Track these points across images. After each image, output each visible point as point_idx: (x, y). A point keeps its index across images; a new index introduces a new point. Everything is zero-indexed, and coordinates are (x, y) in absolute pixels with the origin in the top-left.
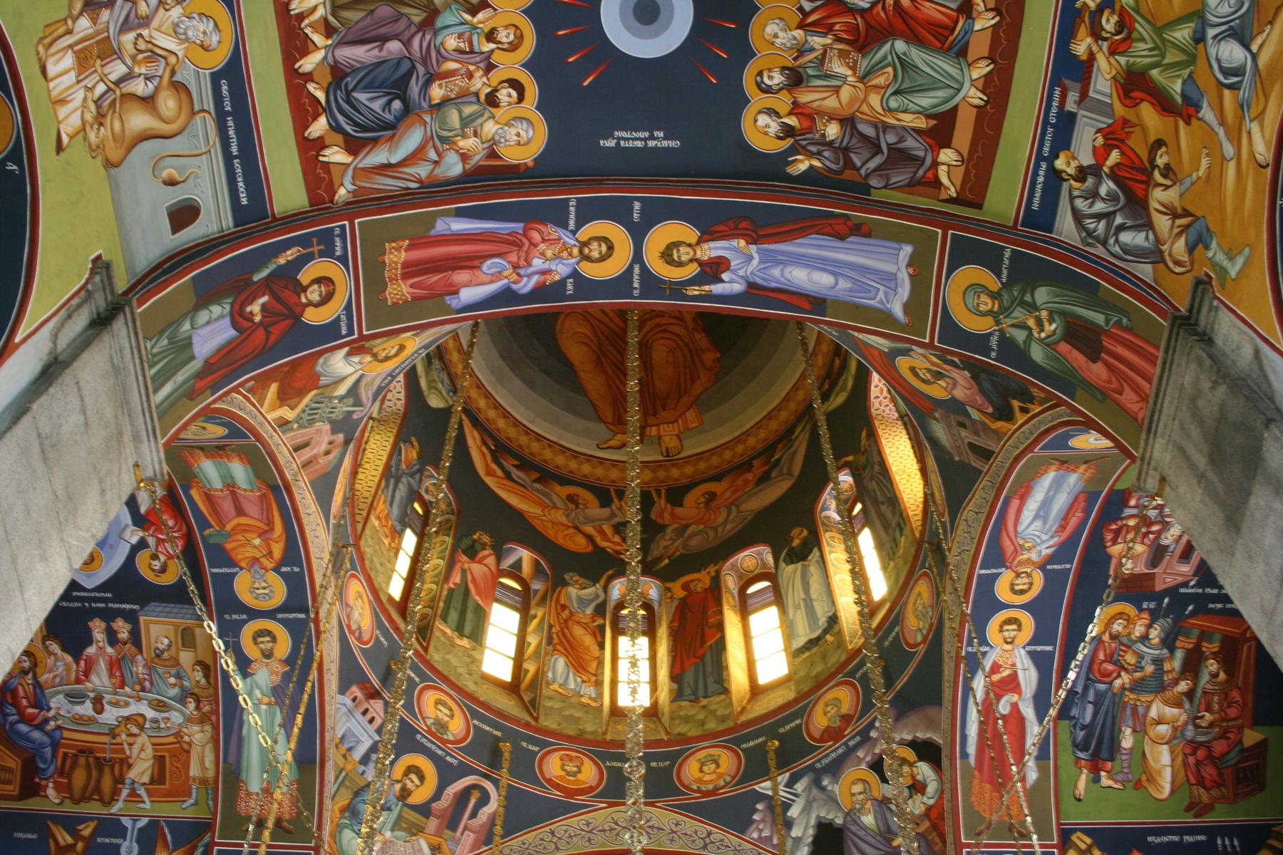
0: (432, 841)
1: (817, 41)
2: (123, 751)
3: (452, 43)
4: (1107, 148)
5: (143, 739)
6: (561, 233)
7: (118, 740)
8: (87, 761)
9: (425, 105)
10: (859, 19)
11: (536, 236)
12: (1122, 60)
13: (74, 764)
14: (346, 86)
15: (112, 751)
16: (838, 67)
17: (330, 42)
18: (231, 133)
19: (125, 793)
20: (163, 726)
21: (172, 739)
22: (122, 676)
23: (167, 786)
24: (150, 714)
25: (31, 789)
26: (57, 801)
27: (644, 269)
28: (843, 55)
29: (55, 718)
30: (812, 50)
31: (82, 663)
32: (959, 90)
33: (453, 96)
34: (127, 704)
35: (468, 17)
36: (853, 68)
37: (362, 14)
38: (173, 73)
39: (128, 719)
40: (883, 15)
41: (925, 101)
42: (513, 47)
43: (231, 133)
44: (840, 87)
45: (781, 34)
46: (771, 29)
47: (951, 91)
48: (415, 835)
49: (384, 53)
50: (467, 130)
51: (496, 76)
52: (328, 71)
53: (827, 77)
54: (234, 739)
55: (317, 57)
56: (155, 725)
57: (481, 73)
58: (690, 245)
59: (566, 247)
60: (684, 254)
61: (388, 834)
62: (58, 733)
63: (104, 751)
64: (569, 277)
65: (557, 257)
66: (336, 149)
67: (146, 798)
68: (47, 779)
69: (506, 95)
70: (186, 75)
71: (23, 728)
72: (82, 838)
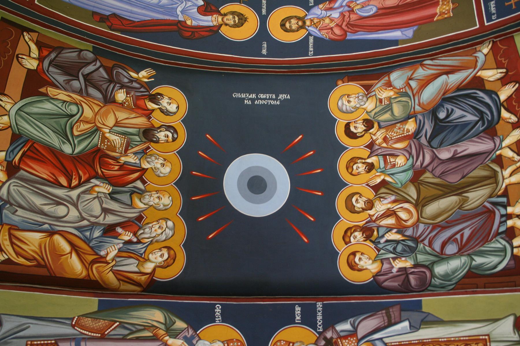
1: (131, 159)
3: (400, 161)
6: (318, 34)
9: (420, 117)
10: (99, 172)
11: (337, 31)
14: (483, 124)
16: (116, 139)
17: (498, 153)
27: (259, 12)
28: (113, 149)
30: (135, 153)
32: (19, 109)
33: (398, 125)
35: (388, 179)
36: (104, 138)
37: (471, 174)
40: (81, 172)
41: (48, 107)
42: (353, 160)
44: (115, 126)
45: (159, 166)
46: (166, 170)
47: (27, 110)
49: (453, 150)
50: (387, 103)
51: (366, 139)
52: (499, 133)
53: (124, 134)
55: (507, 142)
57: (377, 142)
58: (226, 25)
59: (316, 25)
60: (230, 20)
64: (312, 7)
65: (323, 19)
66: (491, 79)
69: (359, 128)
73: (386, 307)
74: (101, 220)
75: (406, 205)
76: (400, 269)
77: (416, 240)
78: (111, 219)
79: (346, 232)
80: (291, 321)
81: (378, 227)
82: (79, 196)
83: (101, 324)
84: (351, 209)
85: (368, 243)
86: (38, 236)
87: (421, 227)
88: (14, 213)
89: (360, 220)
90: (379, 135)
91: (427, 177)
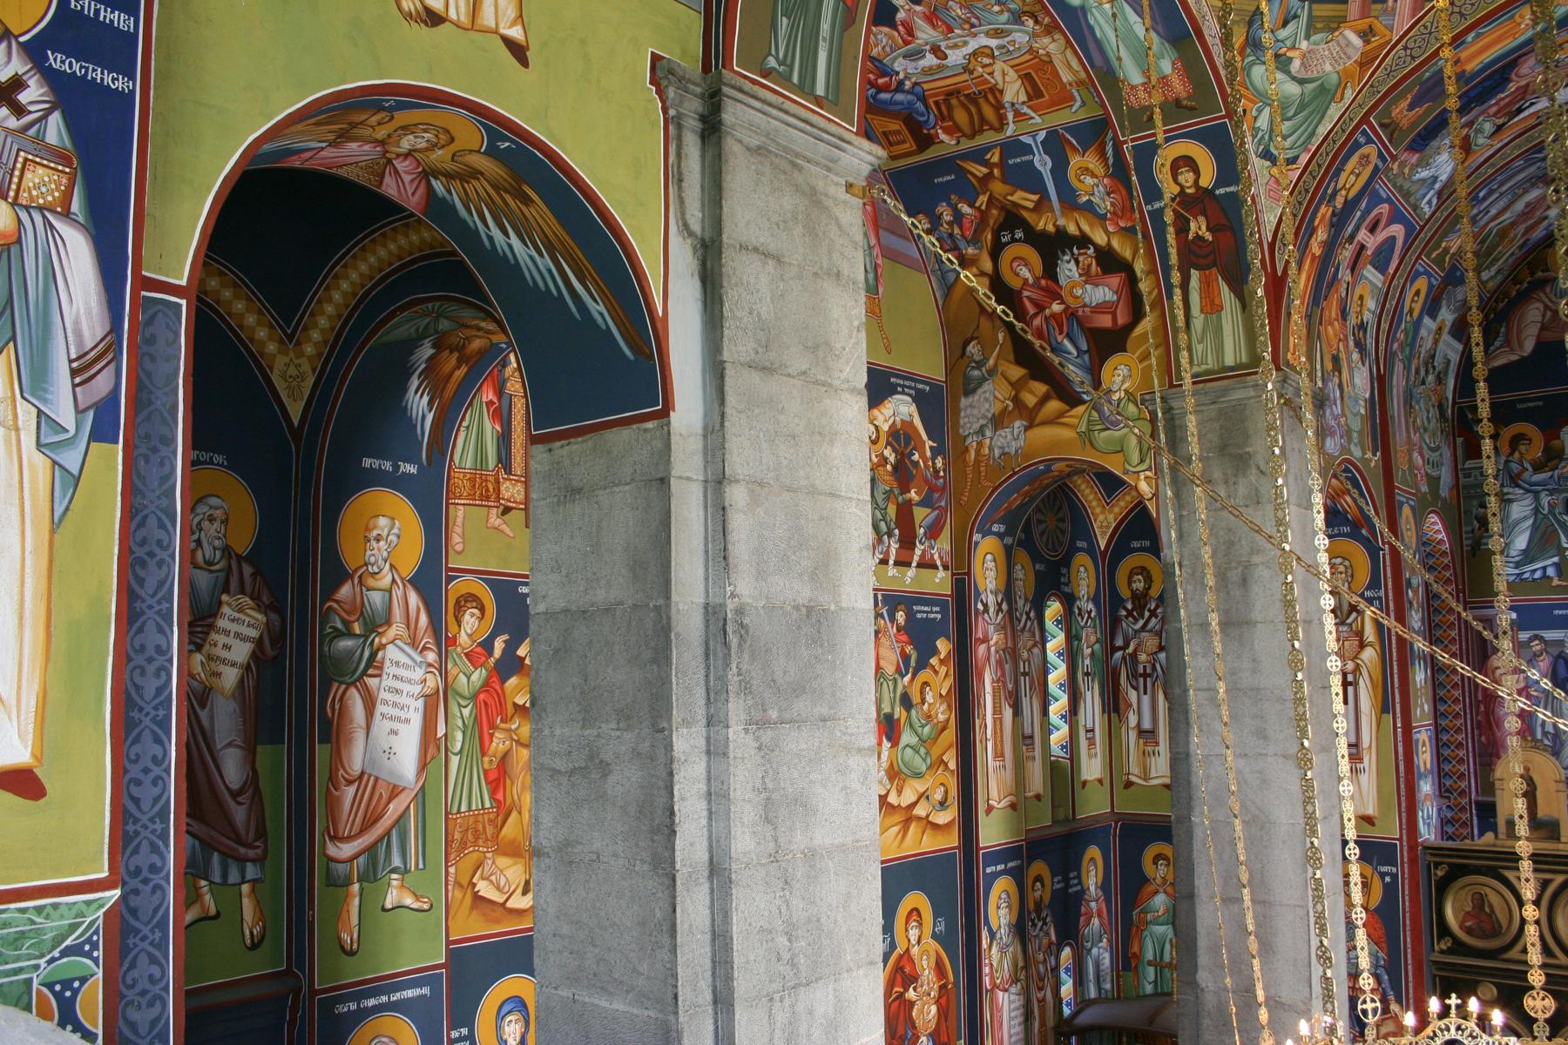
0: (1360, 27)
2: (987, 82)
5: (999, 66)
7: (976, 74)
8: (960, 101)
13: (950, 108)
15: (976, 85)
19: (1010, 116)
20: (1011, 48)
21: (1027, 57)
22: (944, 23)
23: (1047, 97)
24: (993, 43)
25: (925, 142)
26: (953, 142)
29: (907, 77)
31: (900, 28)
34: (965, 43)
39: (975, 54)
48: (1338, 28)
54: (1092, 46)
56: (1004, 51)
61: (1304, 45)
62: (918, 89)
63: (969, 87)
67: (1033, 114)
68: (934, 127)
71: (884, 96)
72: (995, 165)
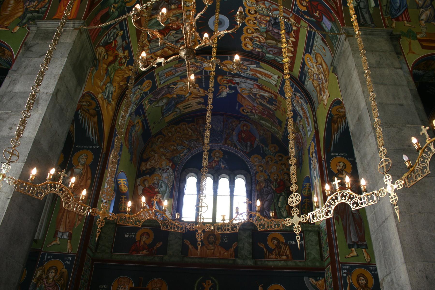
4: (115, 44)
12: (119, 59)
16: (174, 19)
18: (311, 43)
30: (180, 20)
35: (259, 28)
36: (170, 20)
38: (316, 63)
42: (250, 20)
43: (311, 43)
51: (254, 16)
53: (176, 16)
69: (253, 12)
70: (314, 60)
73: (252, 61)
74: (174, 40)
75: (262, 37)
76: (258, 51)
77: (263, 46)
78: (177, 39)
79: (245, 37)
80: (227, 59)
81: (254, 39)
82: (167, 37)
83: (179, 65)
84: (247, 32)
85: (251, 42)
86: (160, 51)
87: (265, 44)
88: (153, 50)
89: (250, 36)
90: (258, 16)
91: (270, 33)
